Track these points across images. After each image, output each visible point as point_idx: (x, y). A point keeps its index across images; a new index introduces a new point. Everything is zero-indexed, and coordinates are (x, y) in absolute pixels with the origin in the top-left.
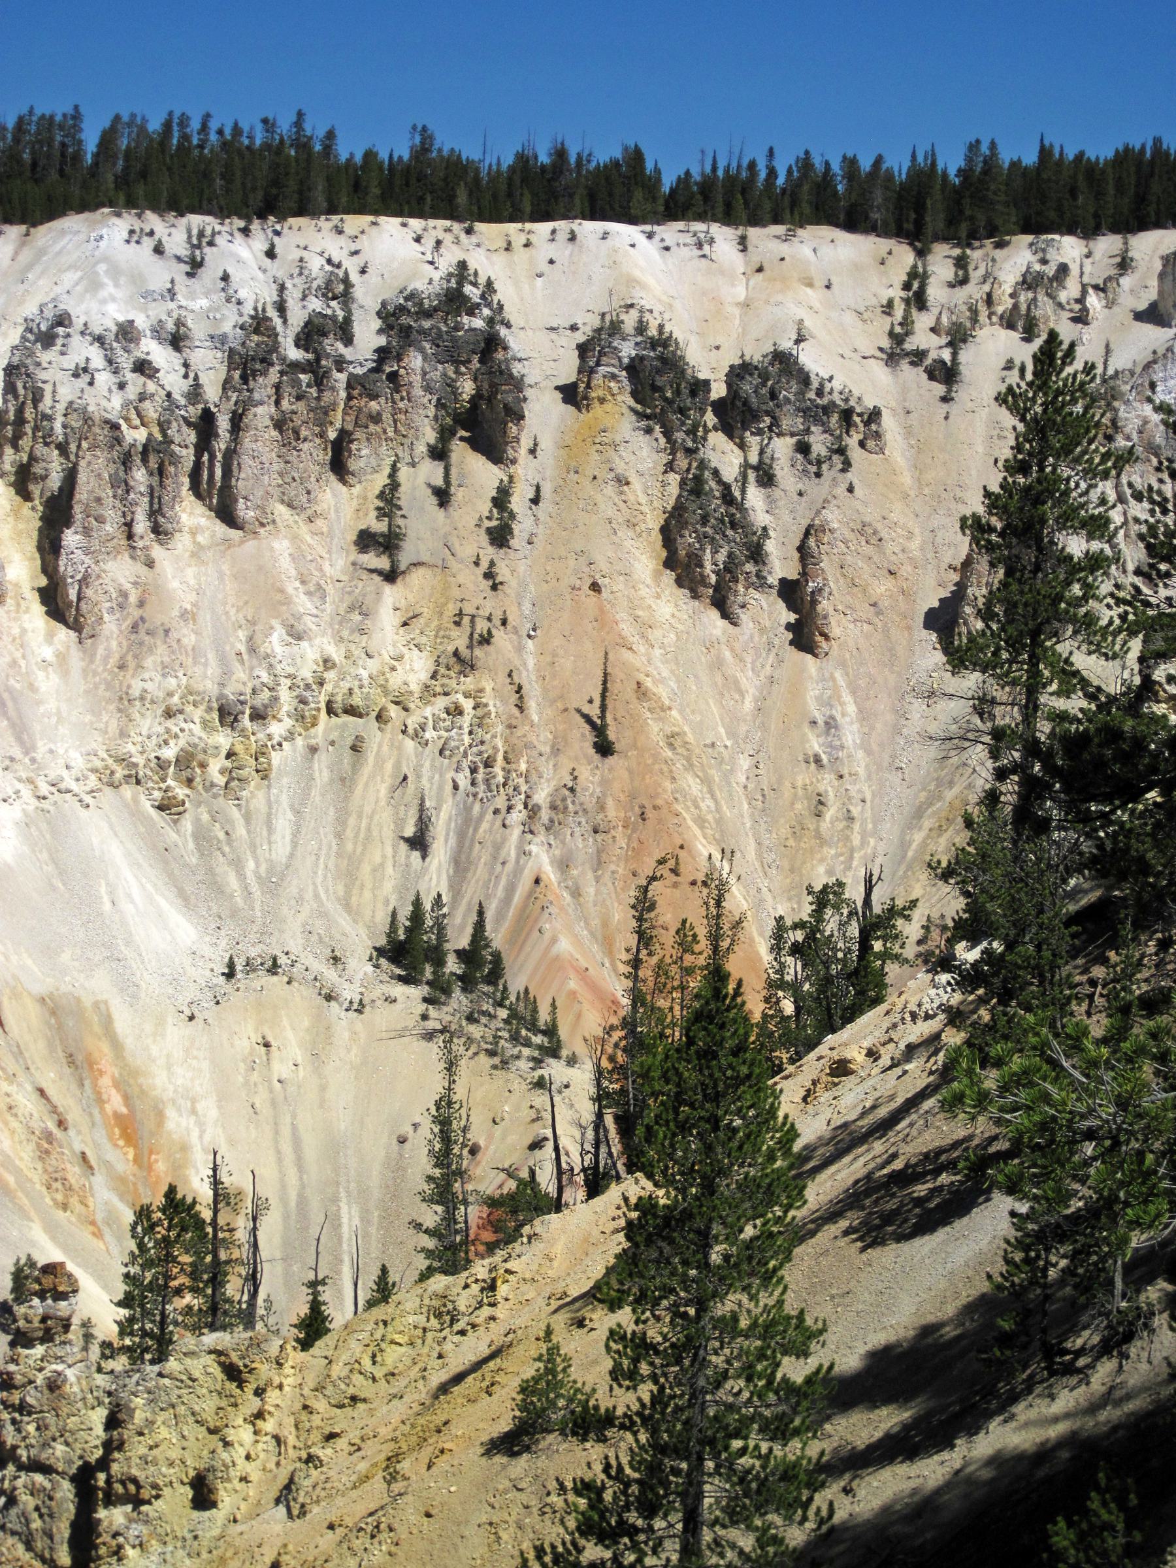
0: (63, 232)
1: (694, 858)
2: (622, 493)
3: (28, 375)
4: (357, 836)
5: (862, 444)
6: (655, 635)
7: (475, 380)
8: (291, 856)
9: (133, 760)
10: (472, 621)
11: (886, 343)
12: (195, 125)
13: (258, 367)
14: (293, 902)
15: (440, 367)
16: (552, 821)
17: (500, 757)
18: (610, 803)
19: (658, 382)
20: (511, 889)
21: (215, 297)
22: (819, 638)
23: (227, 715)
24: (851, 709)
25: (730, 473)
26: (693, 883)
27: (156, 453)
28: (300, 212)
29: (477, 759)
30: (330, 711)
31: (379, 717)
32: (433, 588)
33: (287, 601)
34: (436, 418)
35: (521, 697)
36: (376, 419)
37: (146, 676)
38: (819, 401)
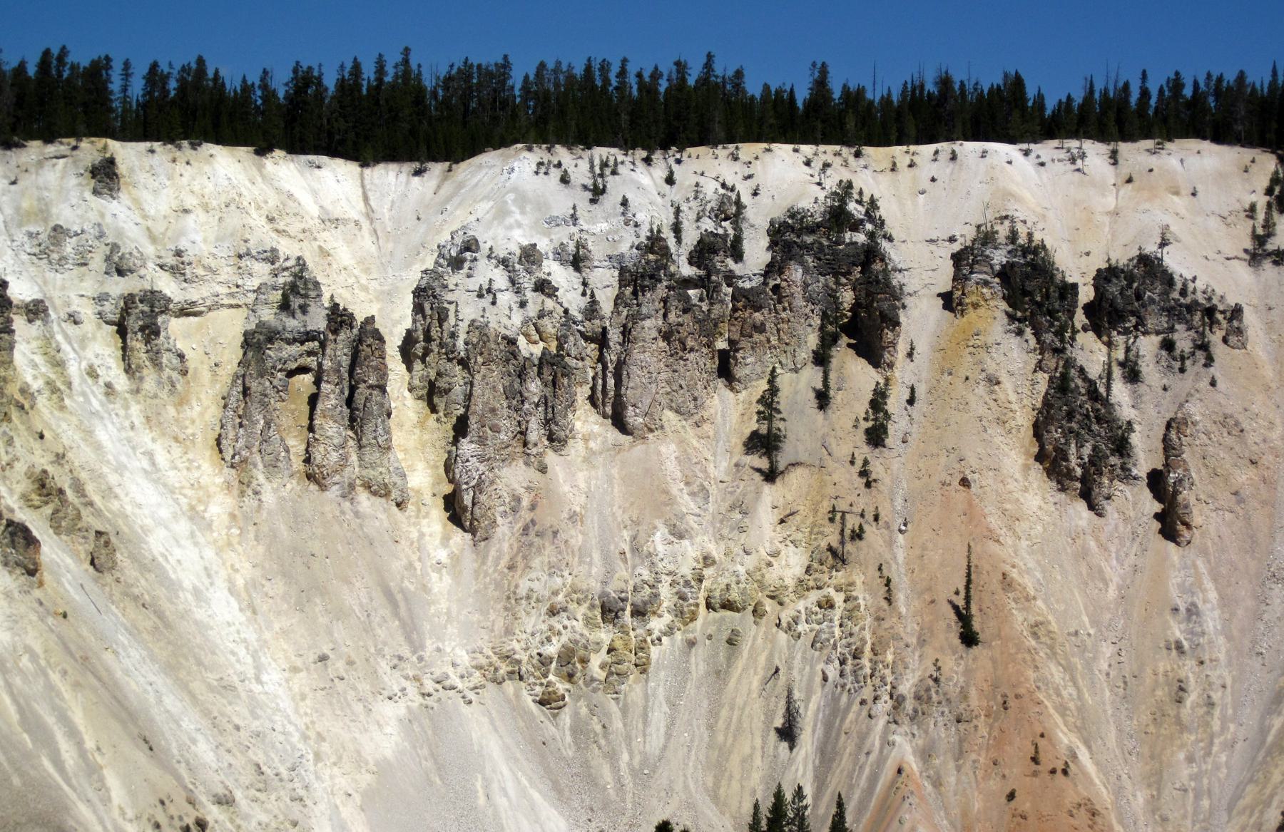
0: (480, 166)
1: (1054, 746)
2: (993, 392)
3: (435, 297)
4: (727, 728)
5: (1225, 340)
6: (1021, 527)
7: (854, 290)
8: (665, 747)
9: (517, 657)
10: (843, 518)
11: (1248, 244)
12: (615, 69)
13: (646, 283)
14: (663, 794)
15: (822, 279)
16: (915, 711)
17: (868, 648)
18: (973, 692)
19: (1027, 285)
20: (873, 779)
21: (614, 221)
22: (1180, 527)
23: (609, 612)
24: (1213, 595)
25: (1094, 371)
26: (1053, 772)
27: (554, 367)
28: (701, 143)
29: (846, 651)
30: (709, 606)
31: (754, 611)
32: (810, 486)
33: (671, 501)
34: (822, 328)
35: (889, 590)
36: (760, 328)
37: (533, 575)
38: (1182, 300)
